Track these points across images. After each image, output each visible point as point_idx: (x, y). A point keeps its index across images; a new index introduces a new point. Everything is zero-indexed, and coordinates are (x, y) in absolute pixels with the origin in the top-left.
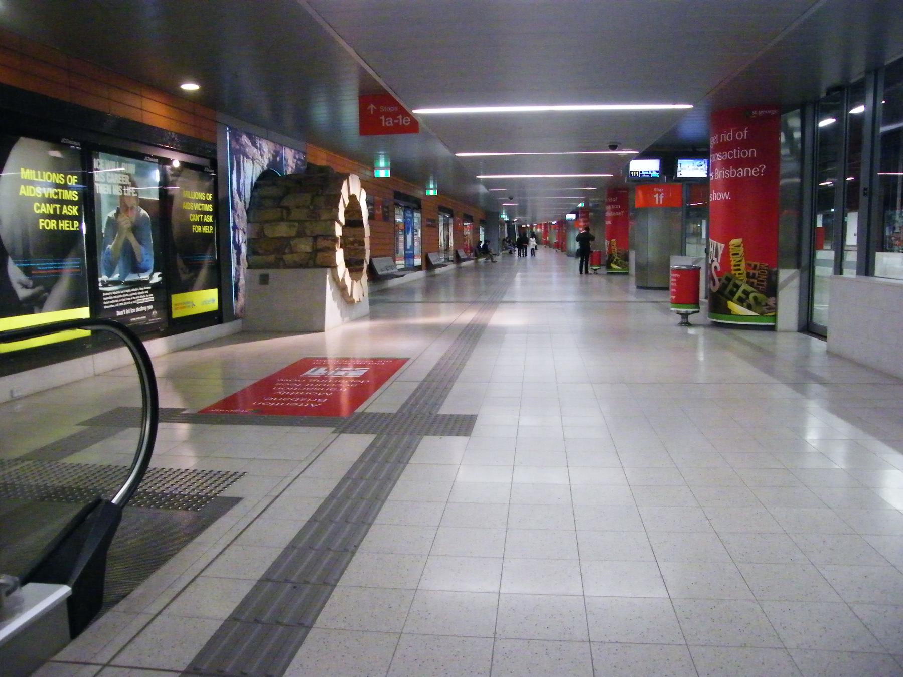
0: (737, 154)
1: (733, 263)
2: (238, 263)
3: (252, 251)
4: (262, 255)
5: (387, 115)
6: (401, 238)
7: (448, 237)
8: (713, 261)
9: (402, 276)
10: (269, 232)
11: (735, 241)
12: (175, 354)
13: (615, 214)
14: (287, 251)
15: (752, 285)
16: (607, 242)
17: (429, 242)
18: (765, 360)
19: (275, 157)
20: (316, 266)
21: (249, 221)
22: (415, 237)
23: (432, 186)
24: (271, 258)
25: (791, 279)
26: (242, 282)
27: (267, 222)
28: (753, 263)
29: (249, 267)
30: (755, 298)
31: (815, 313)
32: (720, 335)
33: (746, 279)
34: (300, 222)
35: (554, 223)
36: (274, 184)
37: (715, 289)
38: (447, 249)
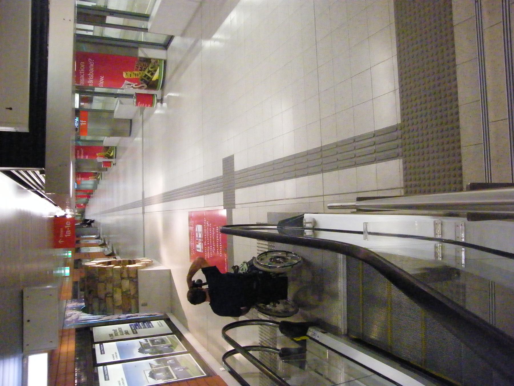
0: (82, 71)
1: (134, 77)
2: (137, 316)
3: (130, 312)
4: (131, 306)
5: (65, 233)
8: (132, 87)
10: (119, 303)
11: (125, 75)
12: (190, 330)
13: (82, 153)
14: (129, 293)
15: (145, 69)
18: (181, 66)
19: (73, 310)
20: (137, 277)
21: (114, 314)
23: (66, 254)
24: (133, 302)
25: (143, 52)
26: (146, 314)
27: (114, 305)
28: (135, 68)
29: (138, 312)
30: (152, 68)
32: (167, 86)
33: (143, 72)
34: (113, 286)
36: (91, 305)
37: (146, 86)
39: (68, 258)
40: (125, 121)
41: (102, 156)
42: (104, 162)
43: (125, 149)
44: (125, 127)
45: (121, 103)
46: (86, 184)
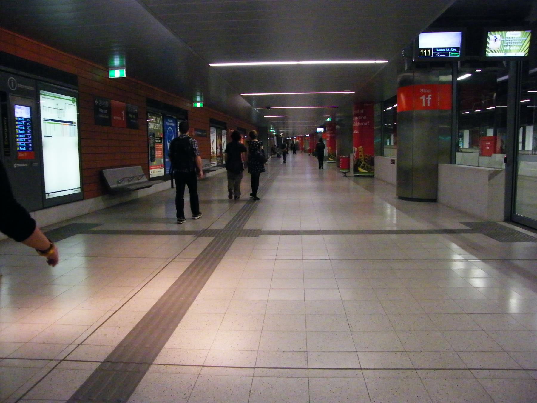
9: (149, 186)
16: (355, 149)
23: (198, 99)
35: (308, 135)
38: (220, 156)
39: (193, 101)
40: (436, 189)
41: (357, 154)
43: (371, 189)
44: (419, 188)
45: (493, 175)
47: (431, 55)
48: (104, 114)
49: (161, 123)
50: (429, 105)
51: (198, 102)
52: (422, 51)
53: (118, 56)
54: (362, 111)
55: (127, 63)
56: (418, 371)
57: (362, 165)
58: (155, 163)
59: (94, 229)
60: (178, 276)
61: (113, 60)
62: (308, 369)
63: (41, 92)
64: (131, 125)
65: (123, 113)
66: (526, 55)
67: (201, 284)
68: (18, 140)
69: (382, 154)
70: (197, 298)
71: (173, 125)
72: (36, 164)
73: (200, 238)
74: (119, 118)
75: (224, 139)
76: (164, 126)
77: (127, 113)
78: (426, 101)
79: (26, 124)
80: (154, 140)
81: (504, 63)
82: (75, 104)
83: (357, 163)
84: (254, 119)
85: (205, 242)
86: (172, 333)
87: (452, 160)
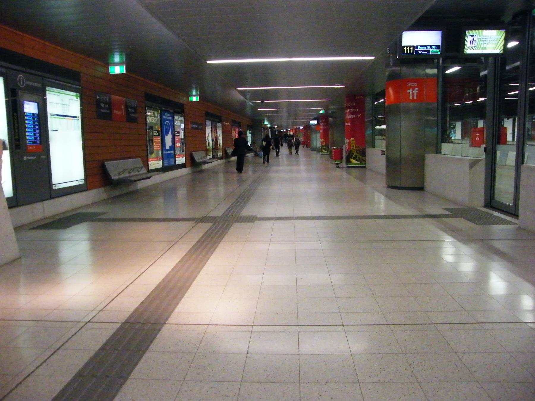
6: (159, 139)
7: (216, 138)
9: (149, 178)
13: (354, 116)
16: (347, 141)
17: (194, 141)
22: (177, 139)
23: (194, 93)
31: (497, 192)
35: (302, 128)
38: (215, 148)
39: (189, 95)
40: (422, 178)
41: (349, 145)
42: (341, 150)
43: (362, 179)
44: (407, 178)
45: (473, 164)
46: (316, 138)
47: (413, 53)
48: (105, 109)
49: (159, 116)
50: (415, 98)
51: (194, 96)
52: (405, 48)
53: (118, 53)
54: (354, 104)
55: (126, 60)
56: (390, 326)
57: (354, 156)
58: (153, 155)
59: (98, 218)
60: (183, 256)
61: (113, 57)
62: (298, 325)
63: (47, 88)
64: (131, 120)
65: (123, 107)
66: (502, 52)
67: (203, 262)
68: (27, 134)
69: (373, 145)
70: (200, 274)
71: (170, 118)
72: (43, 157)
73: (198, 225)
74: (119, 113)
75: (220, 132)
76: (162, 121)
77: (127, 107)
78: (413, 94)
79: (34, 119)
80: (153, 133)
81: (483, 59)
82: (79, 99)
83: (349, 154)
84: (249, 111)
85: (206, 227)
86: (180, 300)
87: (438, 151)
